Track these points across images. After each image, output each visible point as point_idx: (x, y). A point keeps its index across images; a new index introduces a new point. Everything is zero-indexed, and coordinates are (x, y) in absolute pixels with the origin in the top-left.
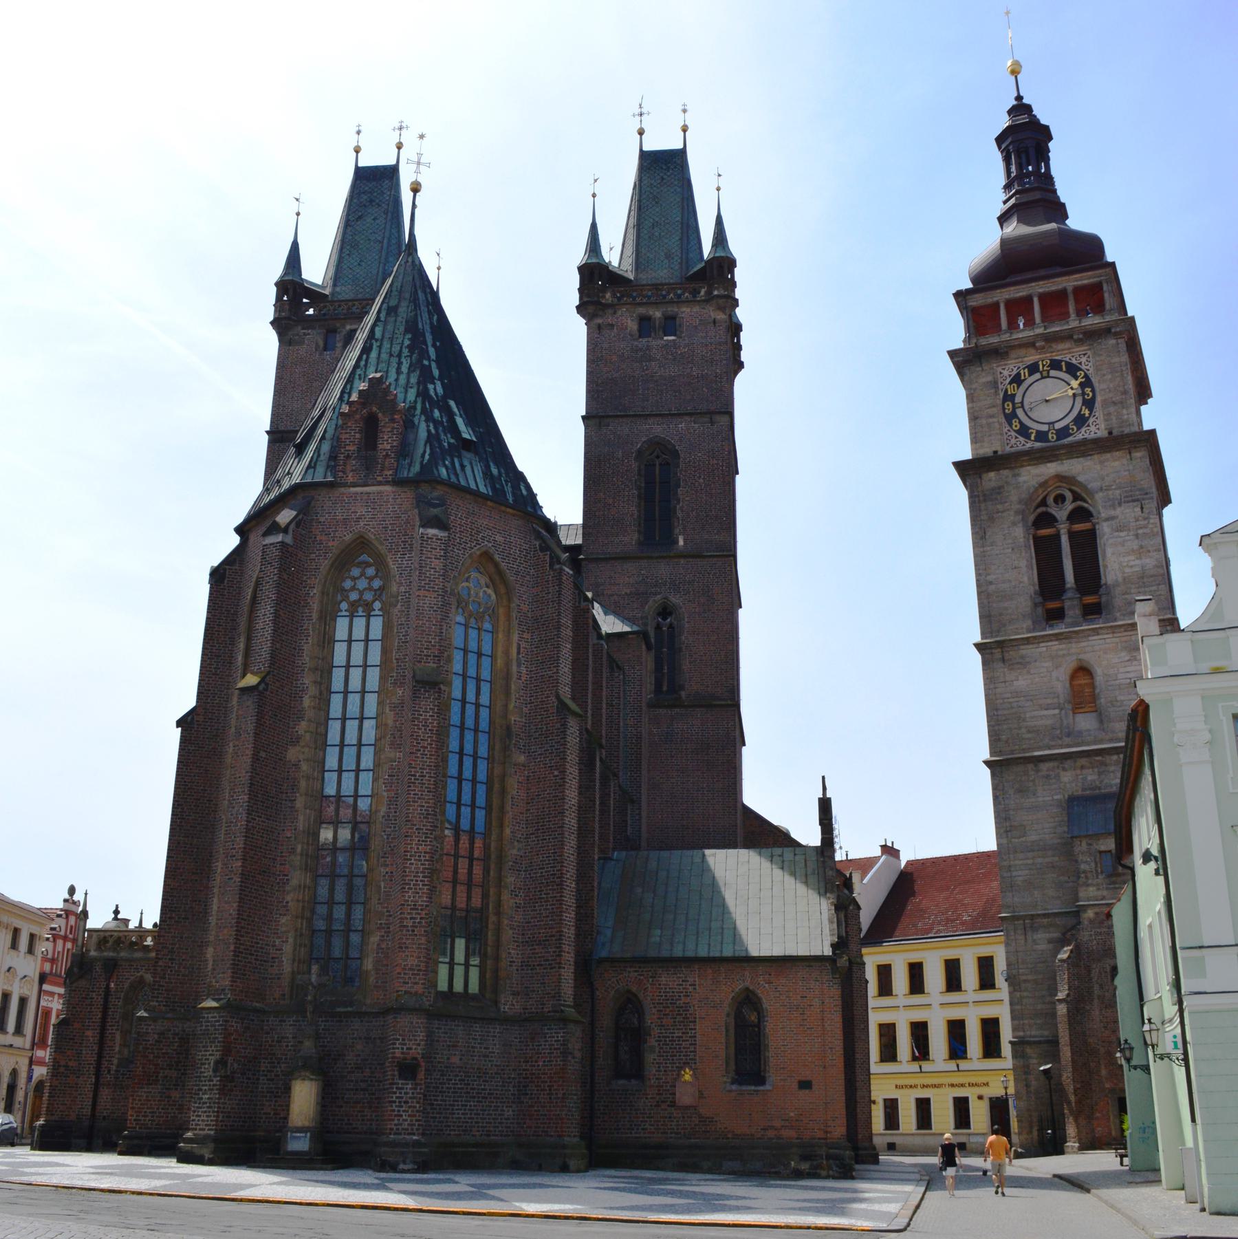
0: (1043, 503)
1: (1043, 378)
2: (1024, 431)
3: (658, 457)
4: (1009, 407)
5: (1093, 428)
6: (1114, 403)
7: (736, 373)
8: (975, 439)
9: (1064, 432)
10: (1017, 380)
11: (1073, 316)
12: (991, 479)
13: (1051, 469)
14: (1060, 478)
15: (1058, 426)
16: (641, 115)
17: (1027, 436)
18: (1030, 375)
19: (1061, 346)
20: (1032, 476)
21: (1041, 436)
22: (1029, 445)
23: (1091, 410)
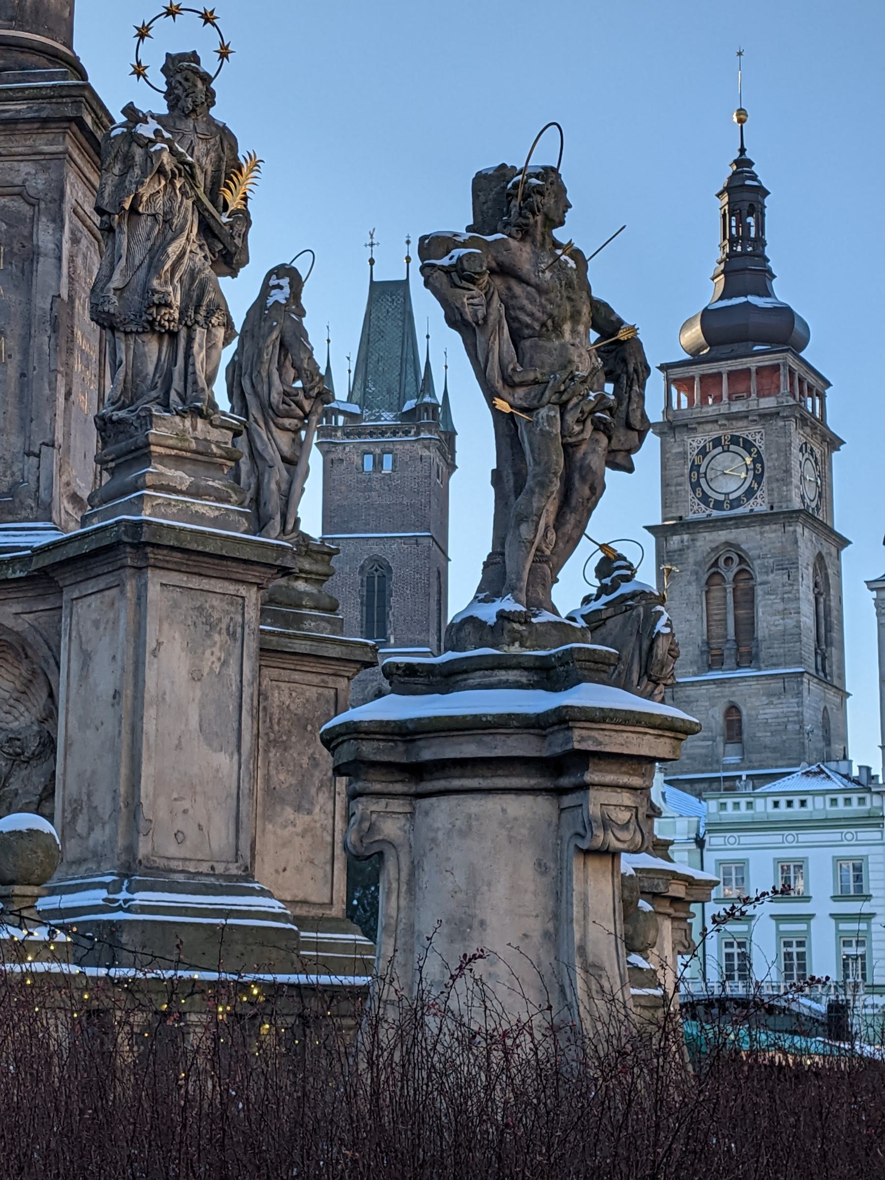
0: (715, 564)
1: (724, 451)
2: (705, 499)
3: (377, 570)
4: (695, 475)
5: (759, 501)
6: (777, 480)
7: (450, 474)
8: (665, 505)
9: (736, 503)
10: (703, 452)
11: (754, 395)
12: (675, 541)
13: (723, 536)
14: (727, 544)
15: (732, 497)
16: (372, 245)
17: (707, 504)
18: (714, 447)
19: (740, 424)
20: (708, 540)
21: (718, 505)
22: (708, 512)
23: (759, 484)
